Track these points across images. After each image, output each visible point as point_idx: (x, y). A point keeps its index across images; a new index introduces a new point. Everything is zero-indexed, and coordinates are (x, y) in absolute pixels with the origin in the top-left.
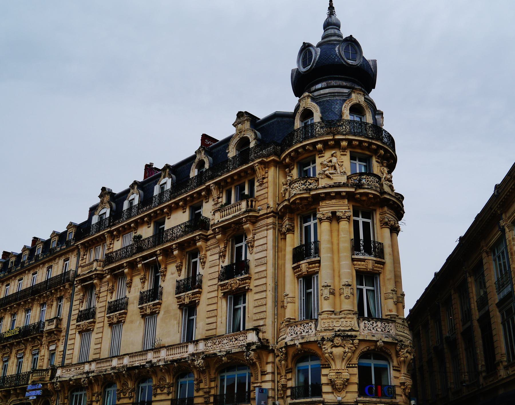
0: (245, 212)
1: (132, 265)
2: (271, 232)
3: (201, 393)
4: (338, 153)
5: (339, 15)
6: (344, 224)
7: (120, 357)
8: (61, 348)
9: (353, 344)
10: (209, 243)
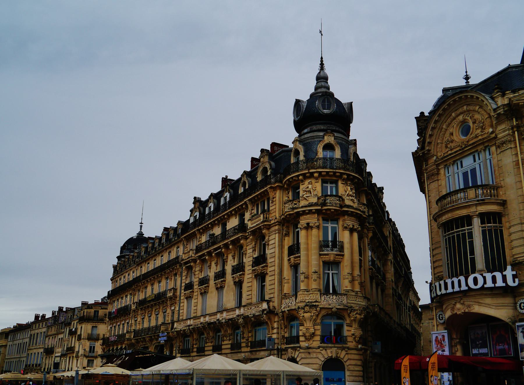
0: (263, 222)
1: (210, 254)
2: (277, 235)
3: (245, 340)
4: (313, 181)
5: (328, 71)
6: (315, 231)
7: (204, 316)
8: (177, 309)
9: (316, 310)
10: (248, 241)
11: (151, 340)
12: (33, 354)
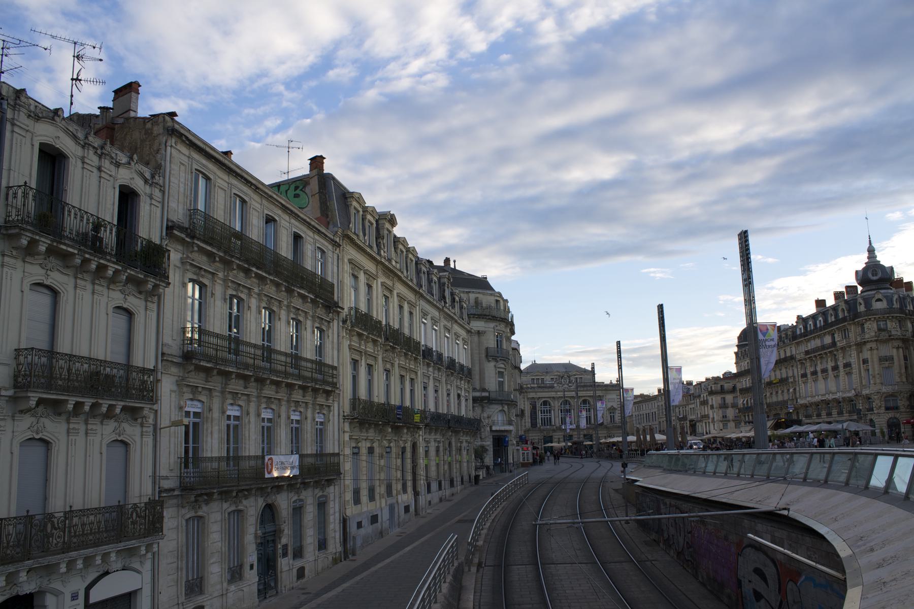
5: (874, 245)
6: (875, 352)
11: (781, 409)
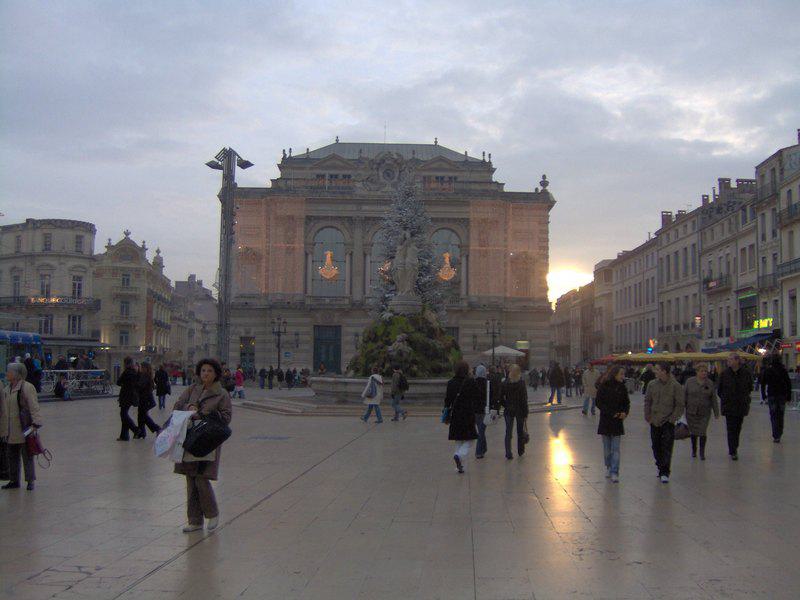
12: (674, 303)
